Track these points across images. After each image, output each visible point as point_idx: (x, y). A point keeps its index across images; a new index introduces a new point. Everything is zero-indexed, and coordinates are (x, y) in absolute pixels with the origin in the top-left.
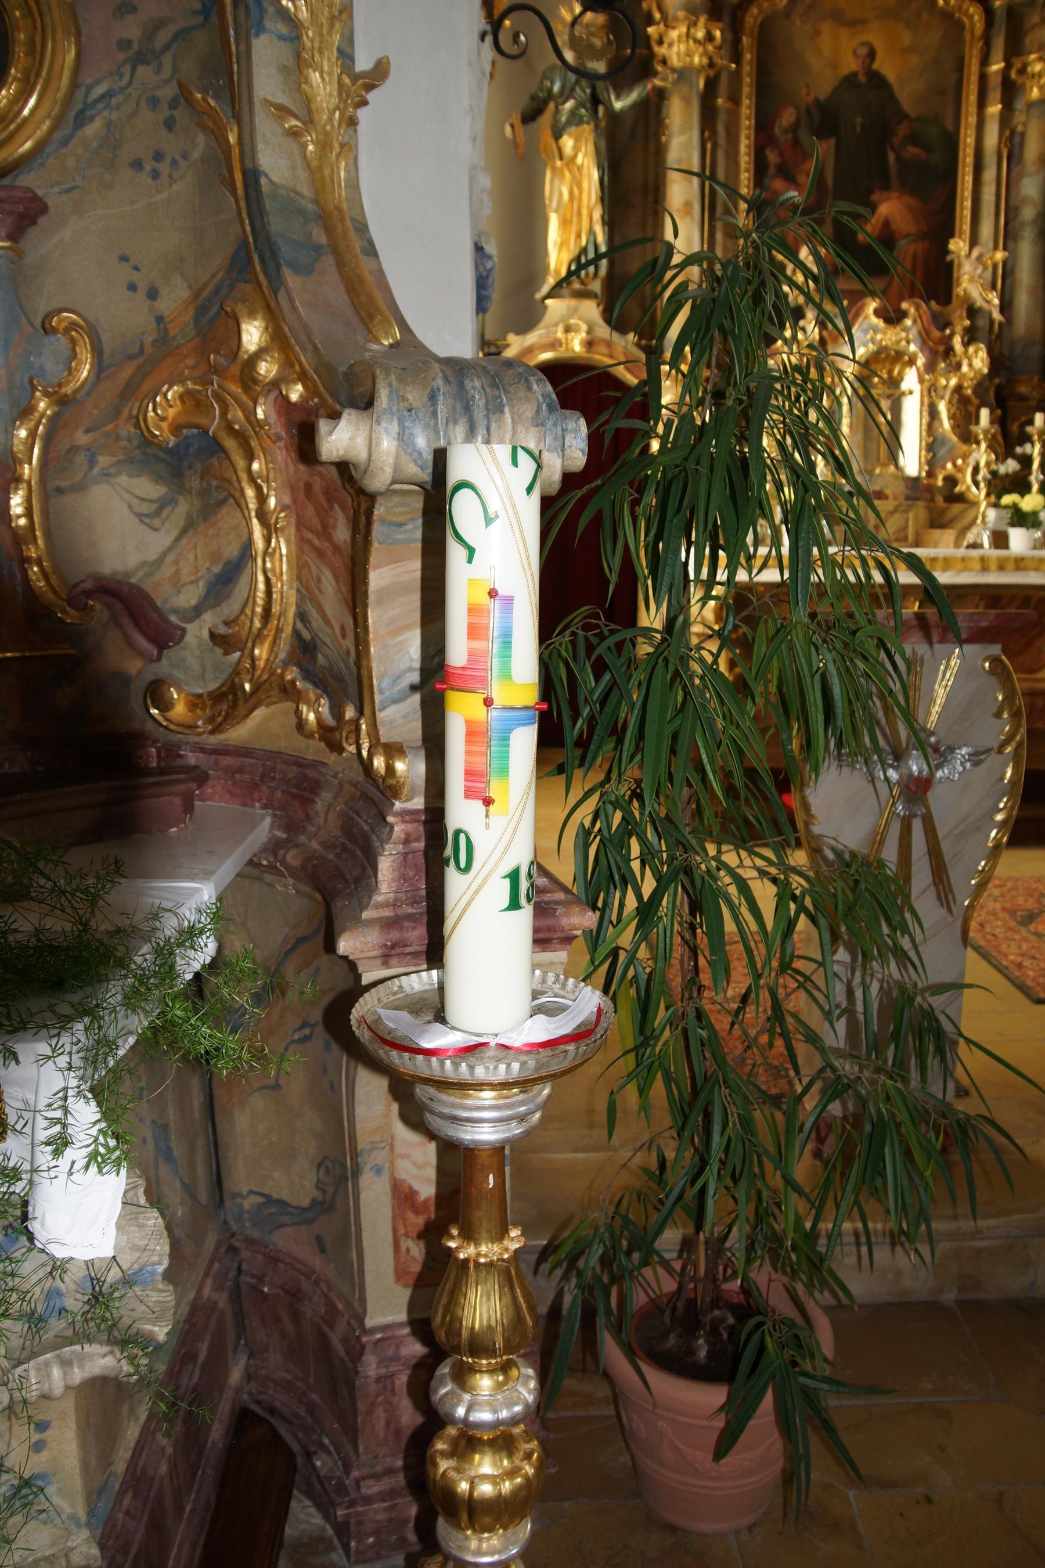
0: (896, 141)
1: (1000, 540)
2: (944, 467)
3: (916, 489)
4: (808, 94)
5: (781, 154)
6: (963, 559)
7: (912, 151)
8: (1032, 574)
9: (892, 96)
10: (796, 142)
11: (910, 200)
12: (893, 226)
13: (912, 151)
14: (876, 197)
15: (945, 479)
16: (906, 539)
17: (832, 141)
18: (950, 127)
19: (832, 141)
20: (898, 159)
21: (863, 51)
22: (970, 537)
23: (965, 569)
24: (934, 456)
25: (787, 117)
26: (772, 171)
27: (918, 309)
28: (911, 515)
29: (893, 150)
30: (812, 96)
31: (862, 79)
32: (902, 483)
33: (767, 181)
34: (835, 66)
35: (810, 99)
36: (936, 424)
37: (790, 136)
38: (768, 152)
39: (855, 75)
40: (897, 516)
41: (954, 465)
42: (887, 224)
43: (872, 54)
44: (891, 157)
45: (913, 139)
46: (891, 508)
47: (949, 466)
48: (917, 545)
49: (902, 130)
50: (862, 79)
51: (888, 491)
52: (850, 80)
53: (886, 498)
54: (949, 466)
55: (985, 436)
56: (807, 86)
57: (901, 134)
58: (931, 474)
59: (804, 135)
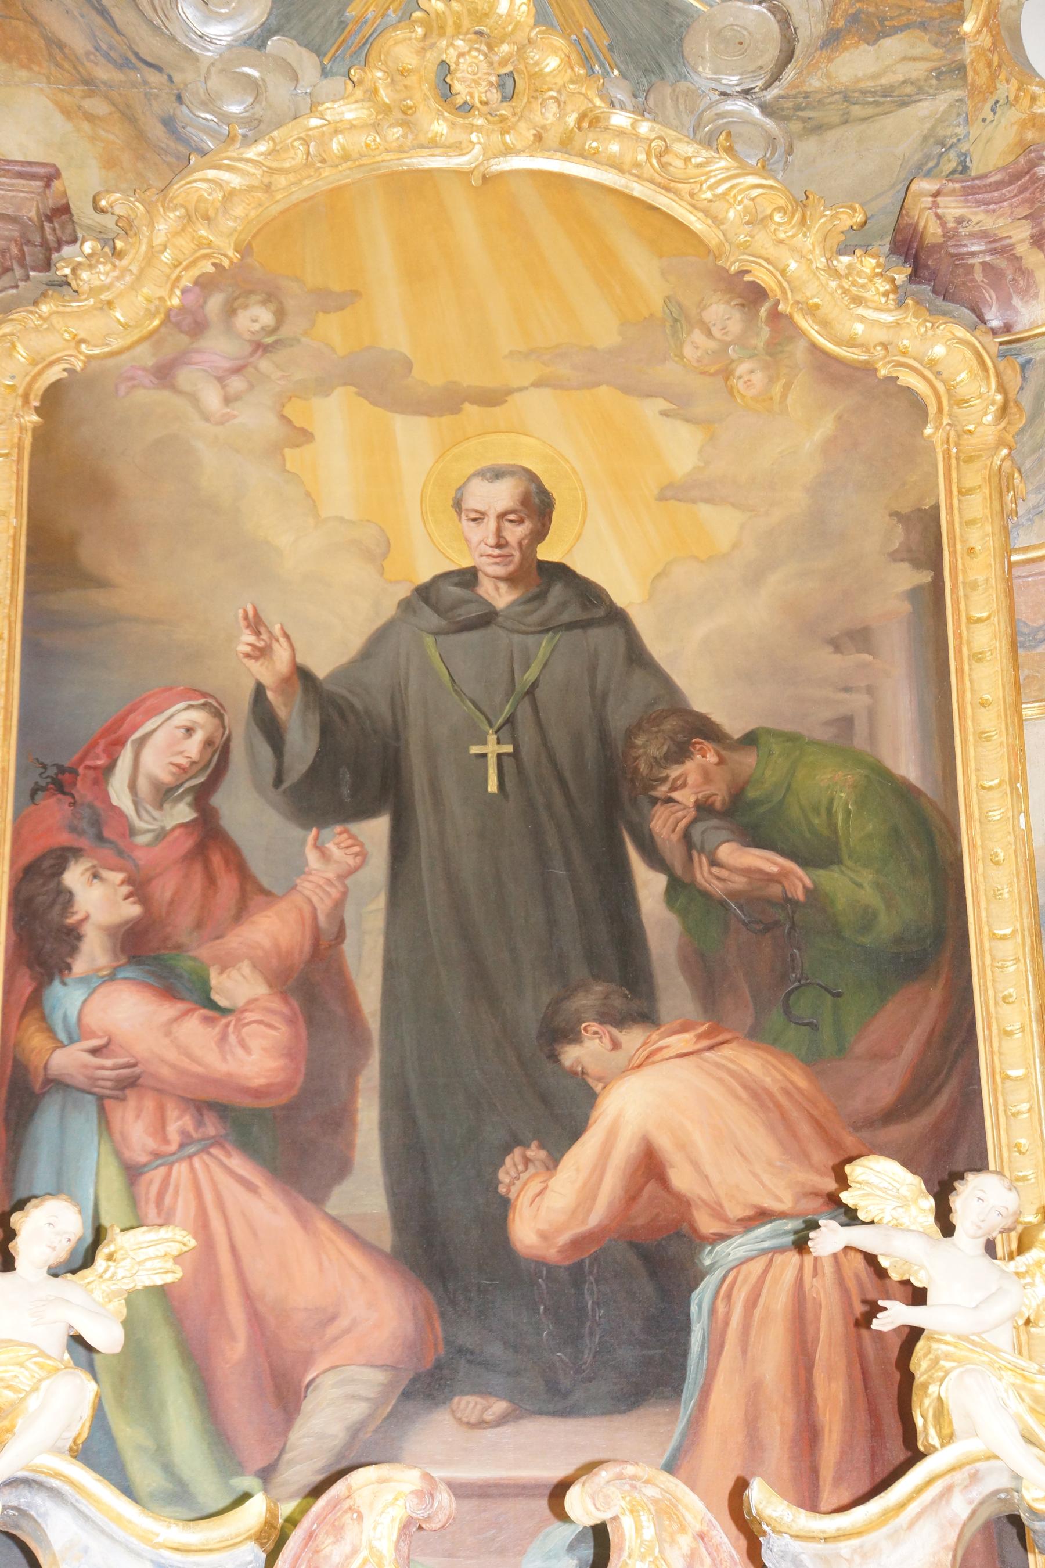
0: (664, 825)
4: (262, 653)
5: (139, 887)
7: (739, 861)
9: (636, 655)
10: (208, 835)
11: (750, 1061)
12: (681, 1179)
13: (738, 862)
14: (588, 1051)
17: (376, 829)
18: (907, 765)
19: (376, 829)
20: (679, 889)
21: (502, 495)
25: (168, 742)
26: (93, 953)
27: (666, 1512)
29: (655, 859)
30: (282, 657)
31: (502, 597)
33: (67, 999)
34: (380, 552)
35: (269, 673)
37: (183, 812)
38: (74, 877)
39: (468, 577)
42: (650, 1166)
43: (537, 507)
44: (650, 886)
45: (744, 815)
49: (694, 778)
50: (502, 597)
52: (445, 602)
56: (256, 624)
57: (686, 797)
59: (248, 811)
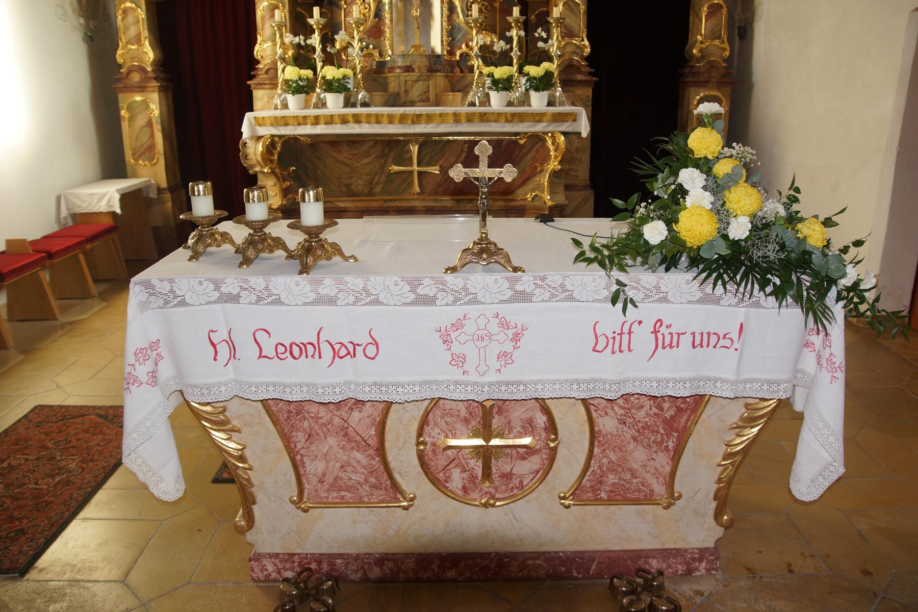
1: (486, 101)
2: (460, 48)
3: (434, 63)
6: (441, 115)
8: (494, 124)
15: (461, 55)
16: (428, 100)
22: (470, 98)
23: (443, 122)
24: (453, 39)
28: (431, 82)
32: (425, 59)
36: (455, 16)
40: (420, 83)
41: (467, 46)
46: (415, 78)
47: (463, 46)
48: (437, 104)
51: (415, 66)
53: (413, 71)
54: (463, 46)
55: (317, 26)
58: (451, 53)
